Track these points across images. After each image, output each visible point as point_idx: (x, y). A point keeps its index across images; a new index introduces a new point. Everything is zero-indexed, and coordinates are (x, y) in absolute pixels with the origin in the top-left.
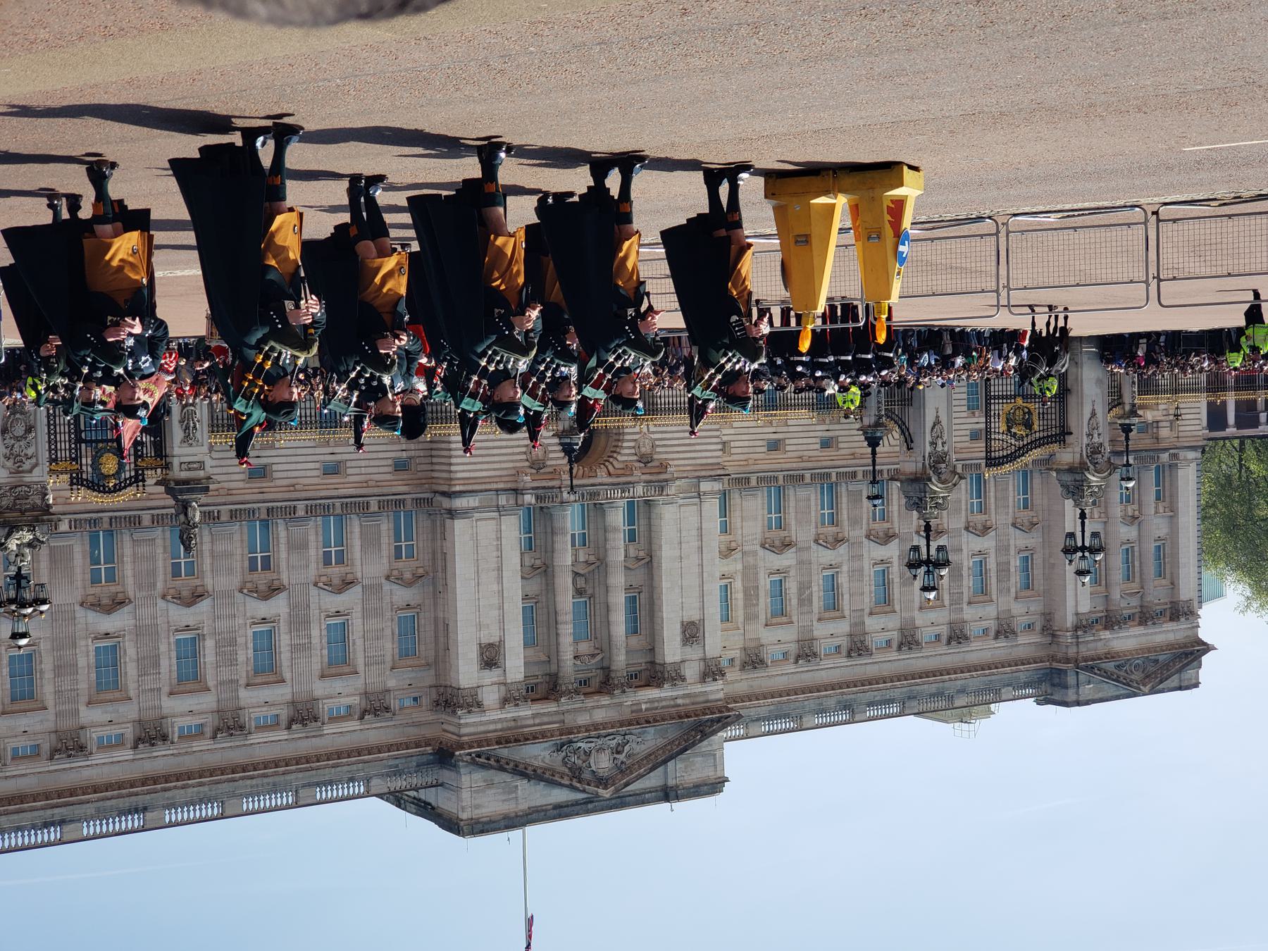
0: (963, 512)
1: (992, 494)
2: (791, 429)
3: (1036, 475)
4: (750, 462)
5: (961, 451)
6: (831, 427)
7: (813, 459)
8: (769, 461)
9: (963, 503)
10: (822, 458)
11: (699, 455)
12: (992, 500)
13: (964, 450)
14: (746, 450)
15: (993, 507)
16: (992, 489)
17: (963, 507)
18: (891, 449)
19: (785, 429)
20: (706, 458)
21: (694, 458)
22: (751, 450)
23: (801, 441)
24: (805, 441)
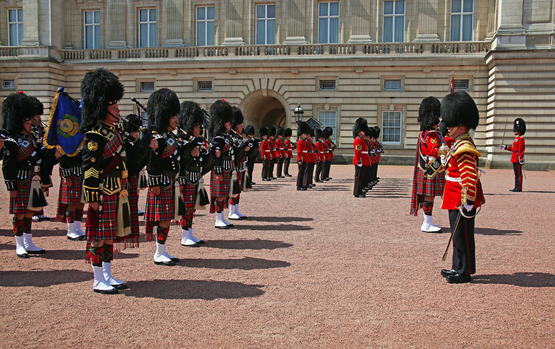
0: (164, 9)
1: (130, 27)
2: (373, 101)
3: (78, 44)
4: (428, 70)
5: (168, 71)
6: (323, 101)
7: (350, 69)
8: (403, 69)
9: (165, 20)
10: (337, 70)
11: (526, 75)
12: (129, 21)
13: (164, 72)
14: (430, 82)
15: (129, 15)
16: (130, 33)
17: (164, 15)
18: (251, 76)
19: (380, 101)
20: (516, 72)
21: (531, 72)
22: (423, 81)
23: (362, 88)
24: (357, 88)
